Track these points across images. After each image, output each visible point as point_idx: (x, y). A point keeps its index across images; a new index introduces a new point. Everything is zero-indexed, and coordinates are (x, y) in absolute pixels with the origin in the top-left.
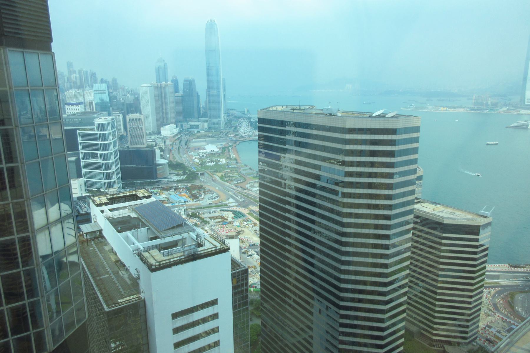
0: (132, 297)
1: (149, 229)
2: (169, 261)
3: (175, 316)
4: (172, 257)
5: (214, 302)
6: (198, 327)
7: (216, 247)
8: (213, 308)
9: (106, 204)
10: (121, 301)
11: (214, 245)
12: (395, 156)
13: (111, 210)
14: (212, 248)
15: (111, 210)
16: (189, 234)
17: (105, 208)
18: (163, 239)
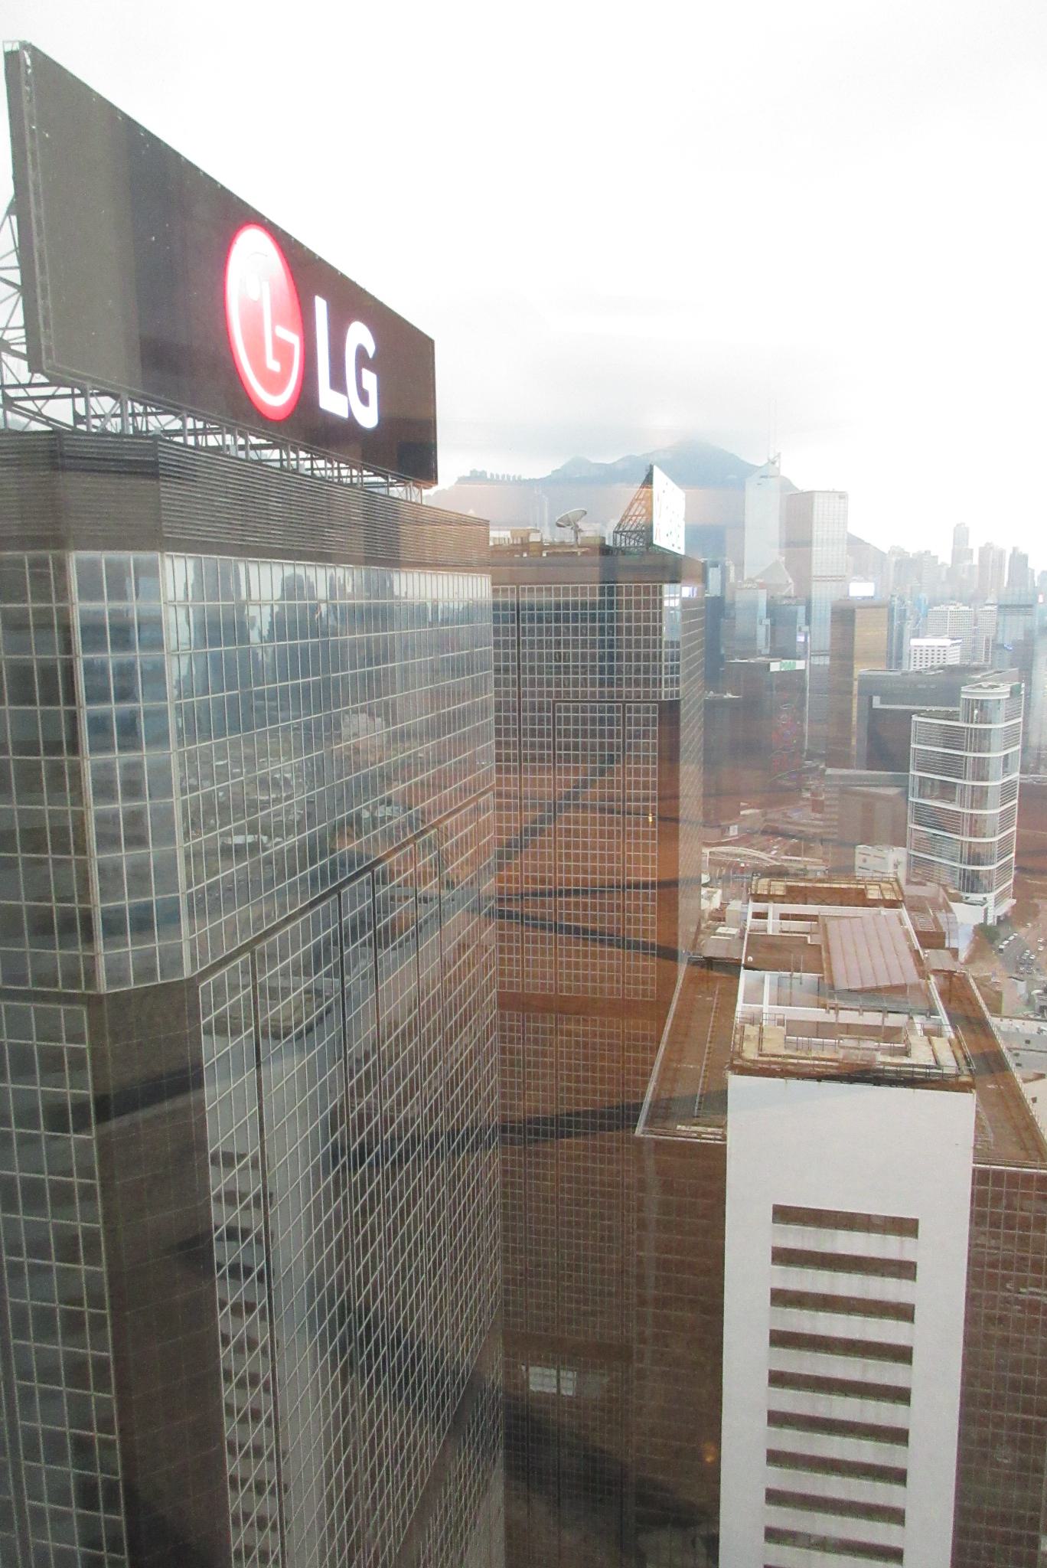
0: (710, 1130)
1: (823, 978)
2: (795, 1061)
3: (784, 1214)
4: (803, 1055)
5: (906, 1227)
6: (847, 1275)
7: (938, 1065)
8: (902, 1242)
9: (781, 899)
10: (684, 1128)
11: (936, 1062)
12: (988, 806)
13: (784, 917)
14: (927, 1067)
15: (784, 917)
16: (911, 1018)
17: (773, 909)
18: (832, 1011)
